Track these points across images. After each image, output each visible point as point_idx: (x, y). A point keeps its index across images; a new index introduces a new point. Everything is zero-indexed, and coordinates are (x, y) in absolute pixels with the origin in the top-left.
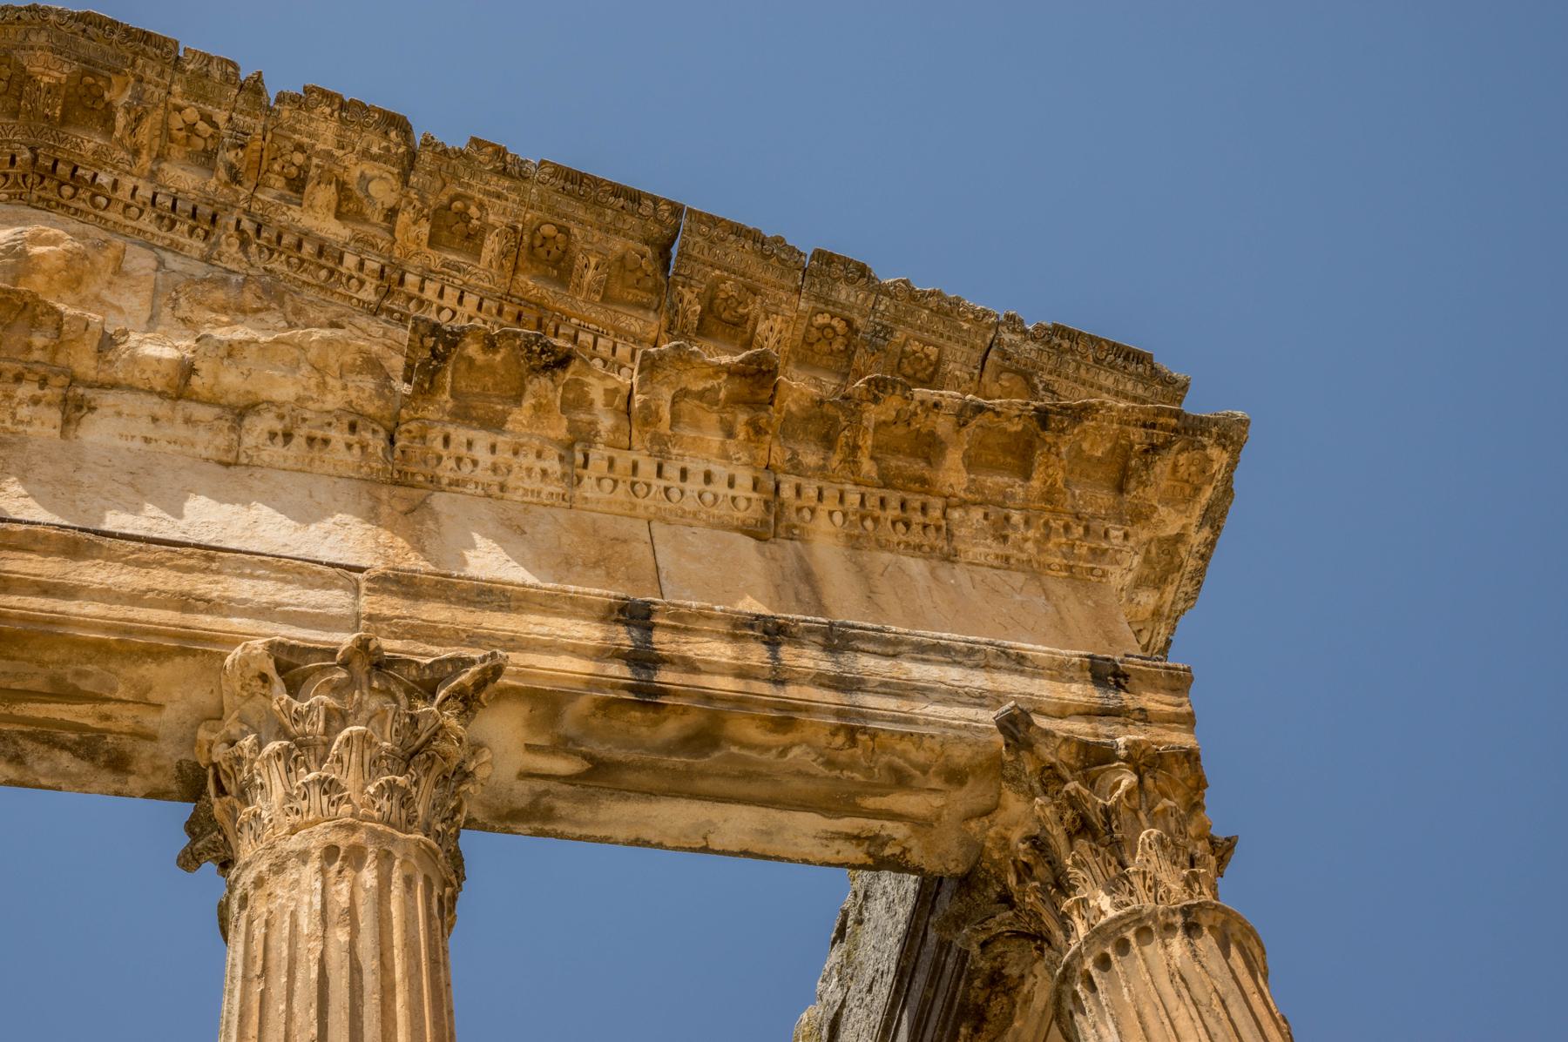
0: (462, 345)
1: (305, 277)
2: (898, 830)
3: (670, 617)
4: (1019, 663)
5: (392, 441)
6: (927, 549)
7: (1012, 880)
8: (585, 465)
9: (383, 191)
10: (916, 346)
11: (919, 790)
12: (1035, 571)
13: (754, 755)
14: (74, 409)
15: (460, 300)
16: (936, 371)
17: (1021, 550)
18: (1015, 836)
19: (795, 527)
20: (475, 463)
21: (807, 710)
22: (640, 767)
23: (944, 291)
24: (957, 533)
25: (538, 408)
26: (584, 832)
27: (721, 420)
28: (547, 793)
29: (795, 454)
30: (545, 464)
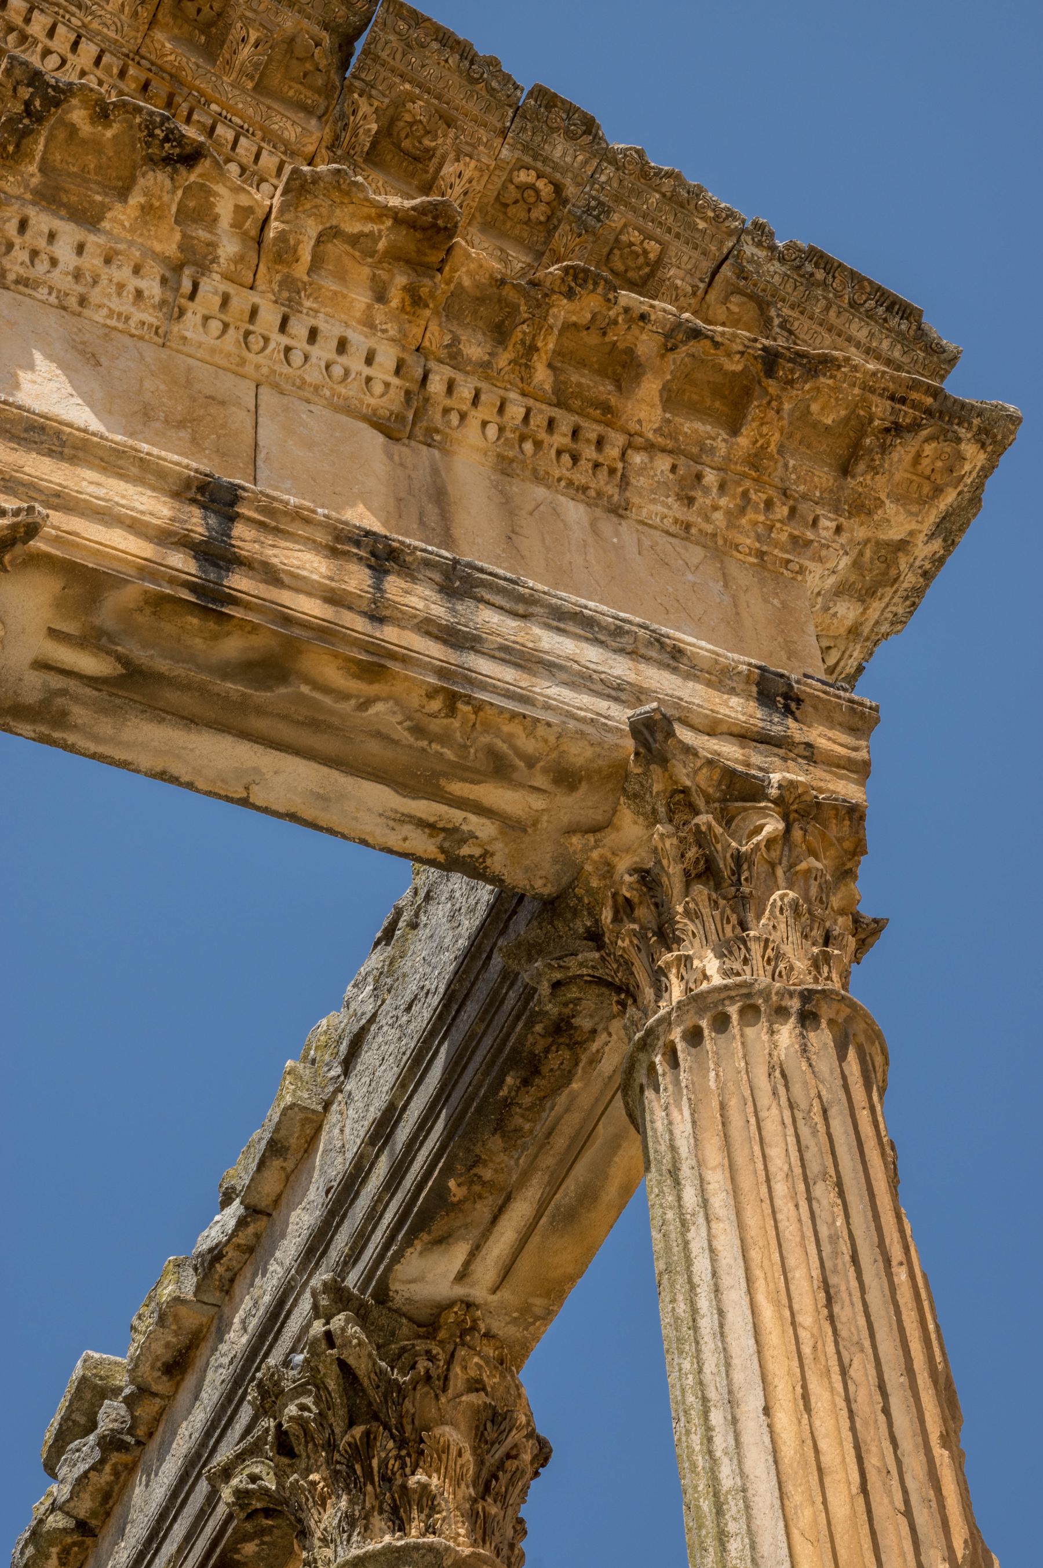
0: (65, 106)
2: (483, 828)
3: (257, 509)
4: (673, 658)
6: (592, 493)
7: (607, 915)
8: (192, 296)
10: (635, 236)
11: (519, 785)
13: (327, 700)
15: (75, 46)
16: (651, 274)
17: (707, 519)
18: (623, 864)
19: (437, 431)
20: (54, 262)
21: (404, 660)
22: (185, 686)
23: (684, 175)
24: (633, 481)
25: (146, 209)
26: (100, 749)
27: (374, 278)
28: (63, 692)
29: (456, 340)
30: (142, 284)
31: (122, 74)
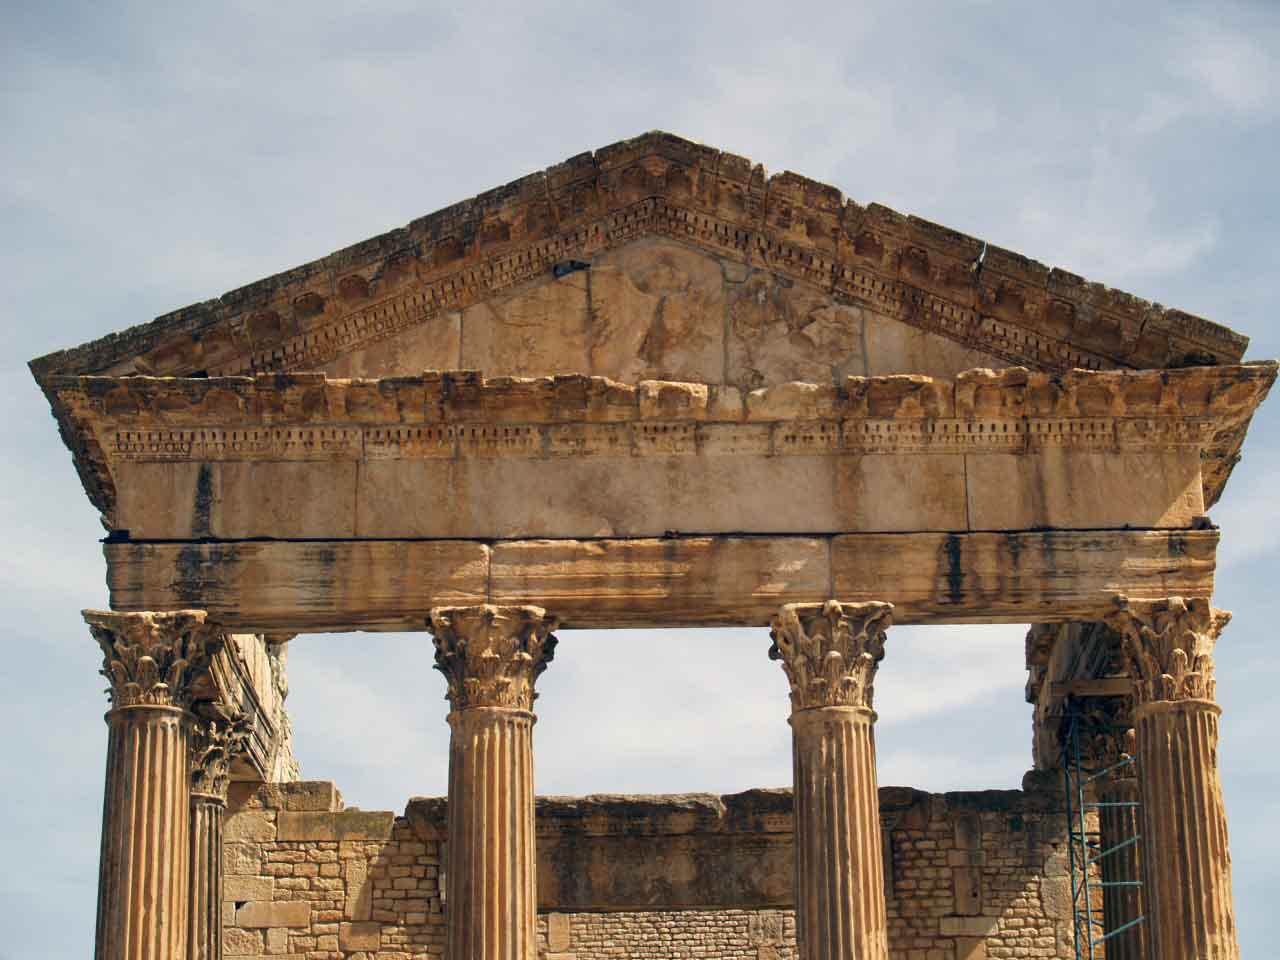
1: (795, 272)
5: (841, 429)
9: (829, 221)
12: (1159, 452)
14: (700, 440)
15: (873, 285)
20: (881, 437)
25: (909, 408)
29: (1037, 409)
31: (893, 290)
